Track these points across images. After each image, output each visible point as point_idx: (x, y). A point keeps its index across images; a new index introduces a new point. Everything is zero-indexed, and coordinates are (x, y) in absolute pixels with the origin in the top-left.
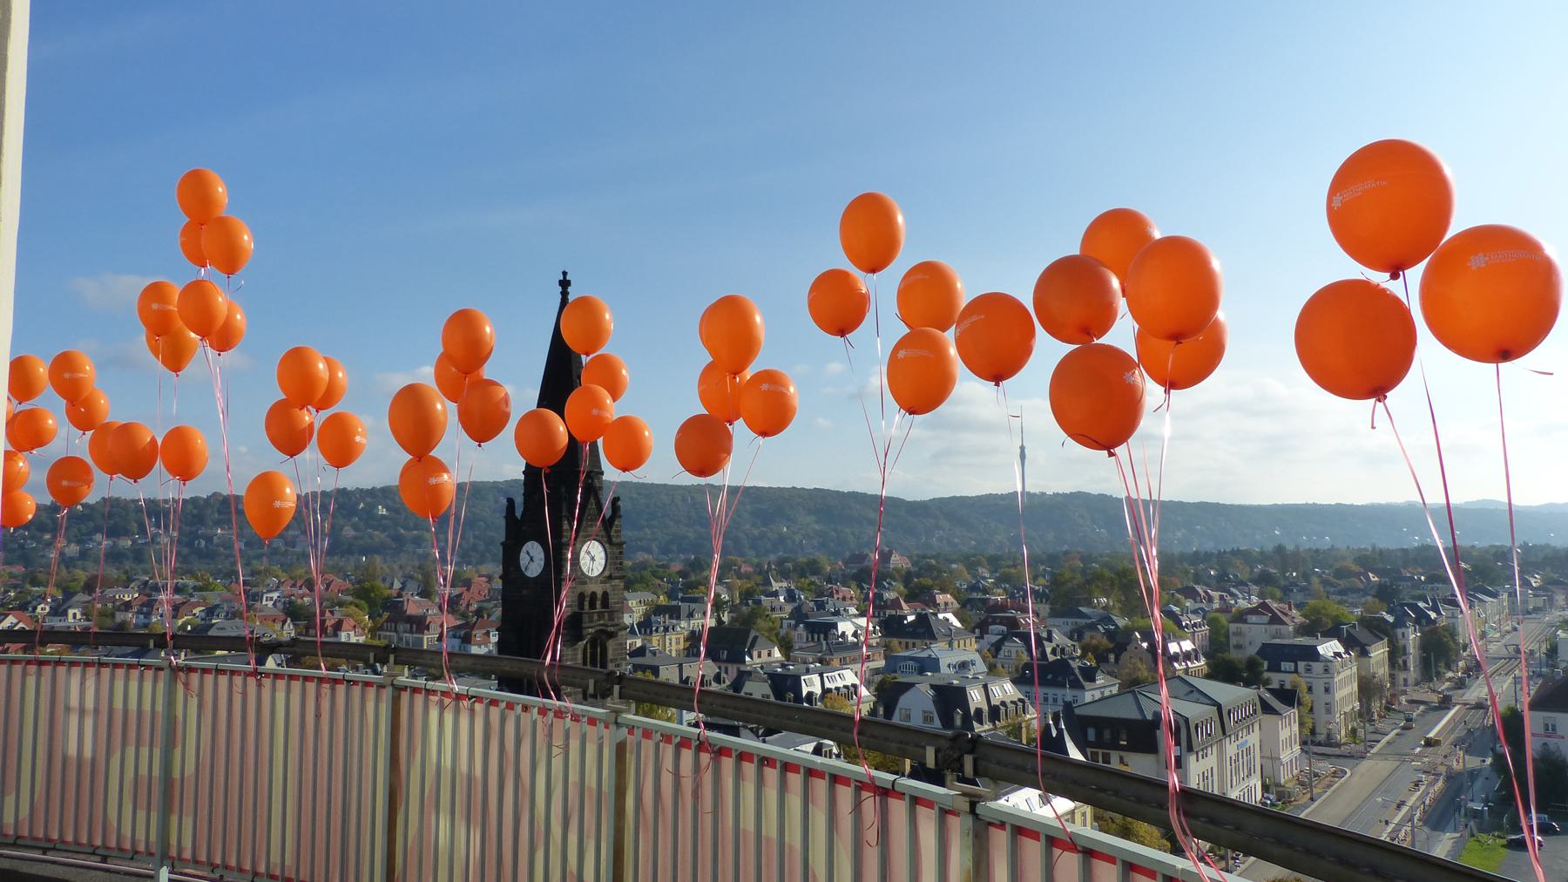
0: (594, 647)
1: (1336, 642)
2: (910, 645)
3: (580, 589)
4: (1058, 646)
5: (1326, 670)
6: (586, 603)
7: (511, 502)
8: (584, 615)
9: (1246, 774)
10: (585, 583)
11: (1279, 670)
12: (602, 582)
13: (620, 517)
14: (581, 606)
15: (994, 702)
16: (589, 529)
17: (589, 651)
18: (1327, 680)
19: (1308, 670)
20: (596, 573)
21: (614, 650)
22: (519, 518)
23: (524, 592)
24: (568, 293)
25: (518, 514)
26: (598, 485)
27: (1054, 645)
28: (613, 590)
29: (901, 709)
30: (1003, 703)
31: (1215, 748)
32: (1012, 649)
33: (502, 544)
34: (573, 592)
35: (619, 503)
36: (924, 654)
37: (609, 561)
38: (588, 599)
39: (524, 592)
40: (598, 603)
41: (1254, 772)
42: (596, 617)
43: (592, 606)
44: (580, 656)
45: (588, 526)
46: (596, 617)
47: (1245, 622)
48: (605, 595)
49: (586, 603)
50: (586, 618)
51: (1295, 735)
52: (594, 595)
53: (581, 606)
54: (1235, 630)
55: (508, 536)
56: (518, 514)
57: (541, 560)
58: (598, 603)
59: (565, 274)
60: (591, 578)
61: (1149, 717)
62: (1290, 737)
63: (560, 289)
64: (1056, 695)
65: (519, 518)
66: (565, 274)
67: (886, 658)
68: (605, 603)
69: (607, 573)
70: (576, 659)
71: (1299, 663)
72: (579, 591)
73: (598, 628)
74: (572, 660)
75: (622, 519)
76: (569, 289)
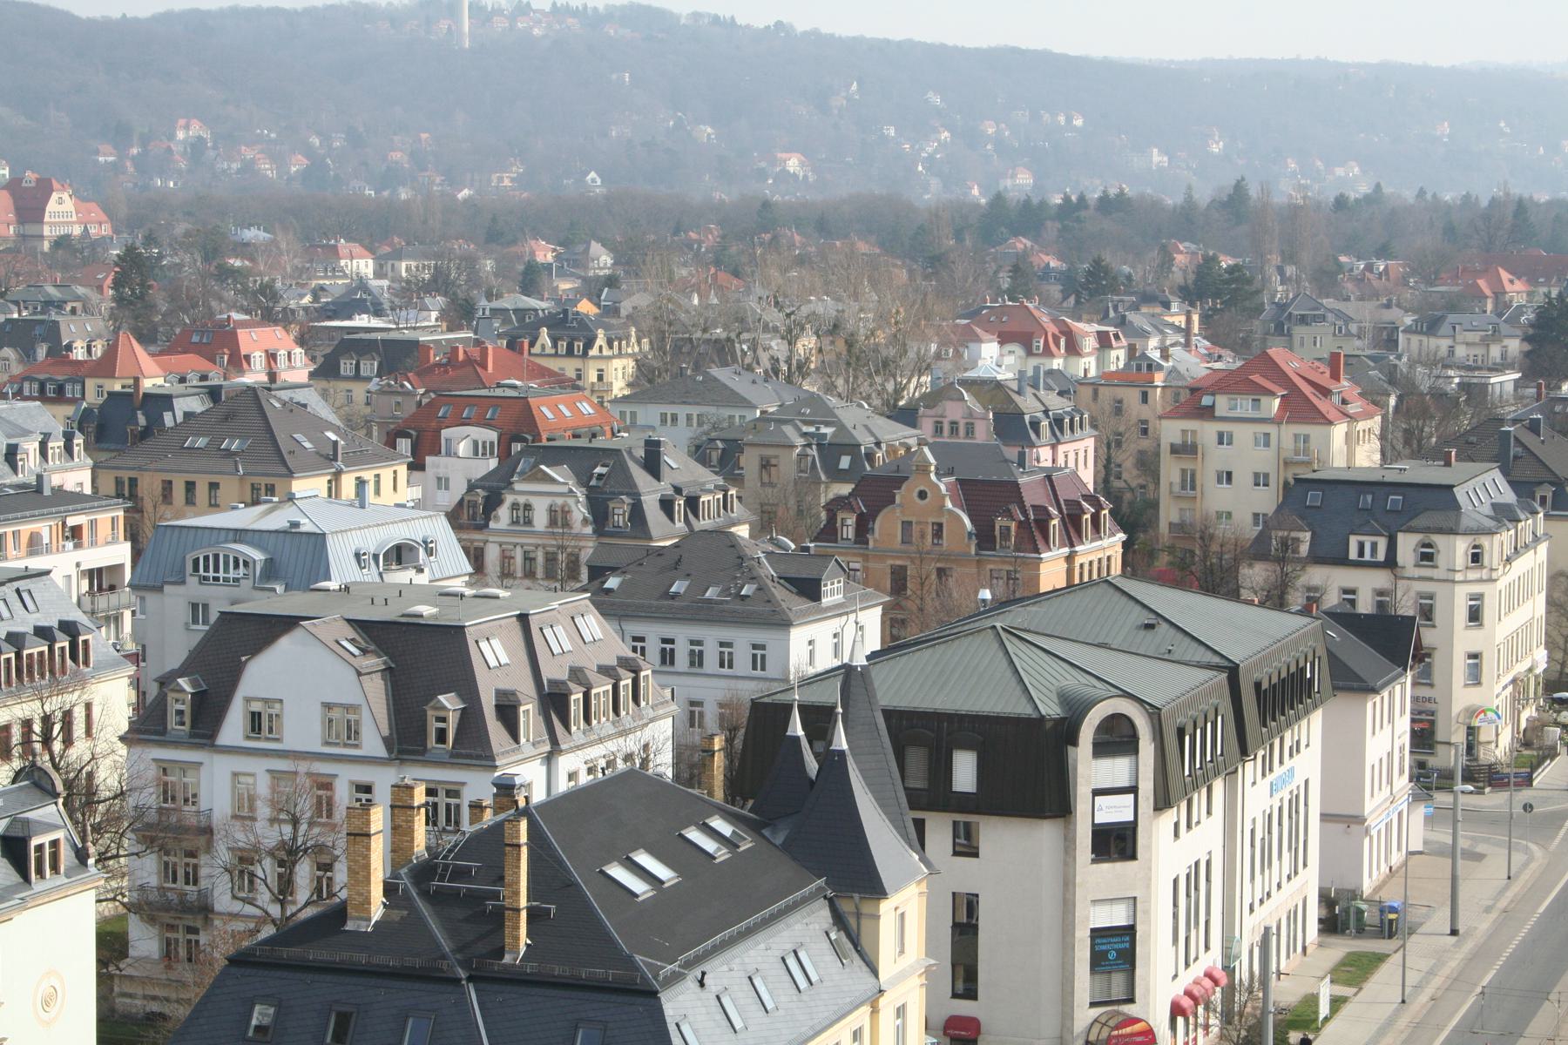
1: (1497, 475)
2: (202, 491)
4: (678, 490)
5: (1476, 558)
9: (1286, 872)
11: (1342, 561)
15: (553, 671)
18: (1476, 589)
19: (1427, 557)
27: (665, 487)
29: (248, 700)
30: (577, 674)
31: (1218, 786)
32: (533, 500)
36: (278, 520)
41: (1305, 865)
47: (1208, 413)
51: (1402, 749)
54: (1178, 440)
61: (1050, 708)
62: (1390, 755)
64: (699, 643)
67: (133, 535)
71: (1401, 537)
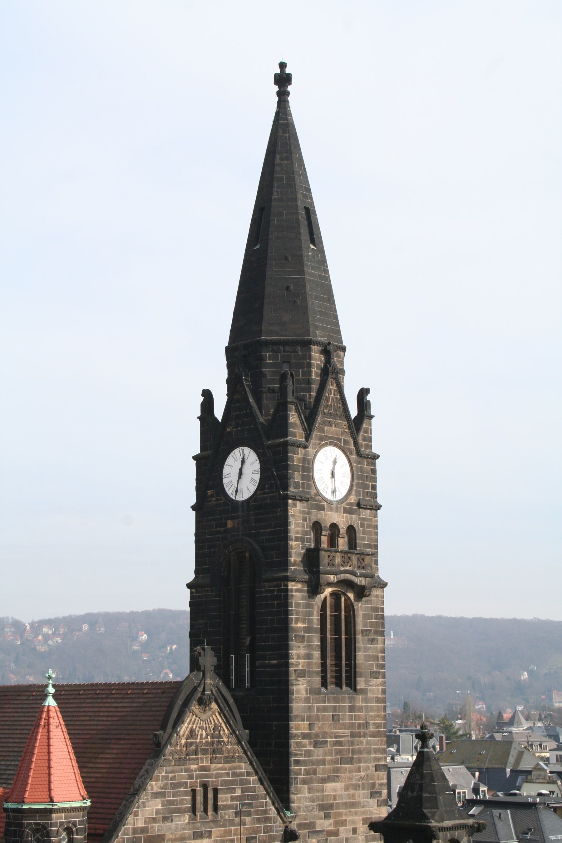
0: (337, 607)
3: (316, 515)
6: (324, 539)
7: (207, 395)
8: (322, 553)
10: (322, 508)
12: (346, 511)
13: (371, 417)
14: (317, 541)
16: (326, 428)
17: (328, 613)
20: (340, 495)
21: (365, 616)
22: (220, 420)
23: (230, 524)
24: (288, 94)
25: (219, 412)
26: (339, 367)
28: (362, 525)
33: (195, 458)
34: (305, 519)
35: (369, 398)
37: (356, 481)
38: (326, 533)
39: (230, 524)
40: (342, 543)
42: (338, 560)
43: (333, 542)
44: (316, 618)
45: (324, 423)
46: (338, 560)
48: (351, 530)
49: (324, 539)
50: (324, 557)
52: (334, 526)
53: (317, 541)
55: (203, 448)
56: (219, 412)
57: (254, 472)
58: (342, 543)
59: (283, 66)
60: (330, 503)
63: (276, 88)
65: (220, 421)
66: (283, 66)
68: (352, 543)
69: (353, 499)
70: (310, 622)
72: (314, 519)
73: (342, 576)
74: (304, 621)
75: (373, 421)
76: (290, 88)
